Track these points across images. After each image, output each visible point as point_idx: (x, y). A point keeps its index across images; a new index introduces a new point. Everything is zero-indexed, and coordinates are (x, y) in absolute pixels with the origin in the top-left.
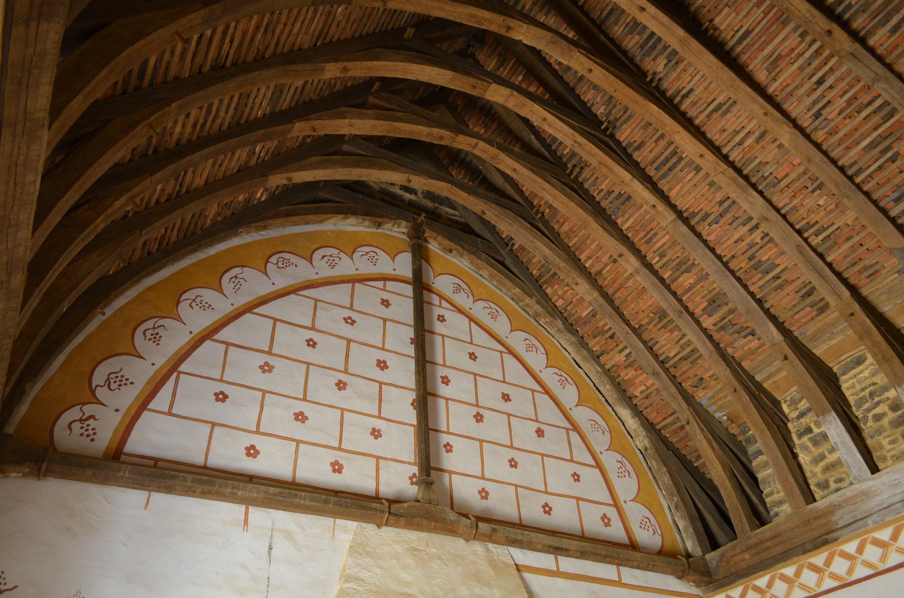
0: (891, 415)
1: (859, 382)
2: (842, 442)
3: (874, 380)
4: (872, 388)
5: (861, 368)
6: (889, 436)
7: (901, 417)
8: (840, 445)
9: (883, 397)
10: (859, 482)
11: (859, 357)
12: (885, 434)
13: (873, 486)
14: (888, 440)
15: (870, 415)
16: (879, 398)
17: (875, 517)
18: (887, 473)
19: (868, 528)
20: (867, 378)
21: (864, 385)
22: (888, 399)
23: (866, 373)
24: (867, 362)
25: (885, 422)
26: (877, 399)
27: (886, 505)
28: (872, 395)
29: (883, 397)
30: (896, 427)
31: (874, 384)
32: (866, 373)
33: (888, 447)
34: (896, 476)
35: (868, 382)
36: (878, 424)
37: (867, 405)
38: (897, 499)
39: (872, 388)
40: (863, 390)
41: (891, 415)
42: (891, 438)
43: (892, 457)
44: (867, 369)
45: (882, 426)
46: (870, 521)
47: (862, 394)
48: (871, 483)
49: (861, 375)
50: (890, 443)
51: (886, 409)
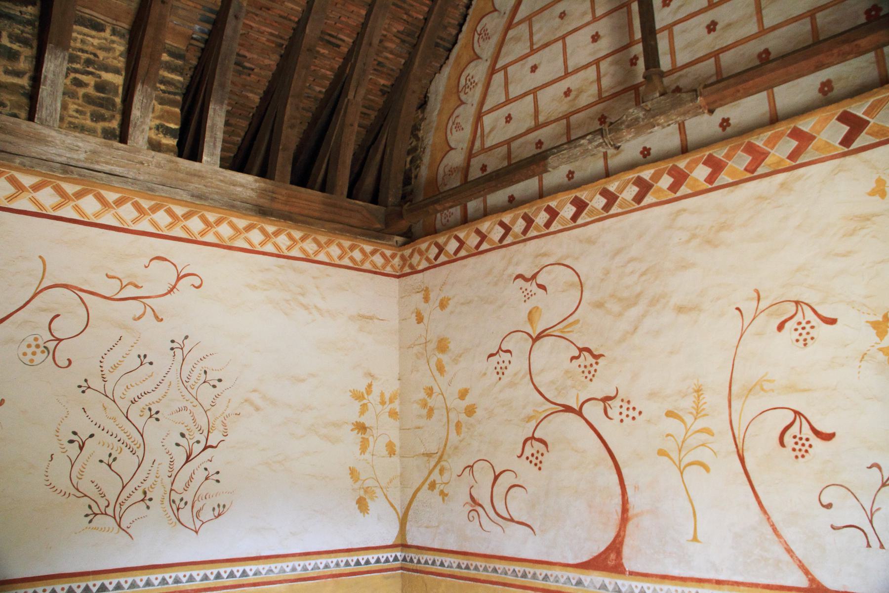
0: (91, 90)
1: (82, 41)
2: (53, 81)
3: (99, 52)
4: (92, 57)
5: (94, 33)
6: (79, 105)
7: (99, 98)
8: (49, 82)
9: (98, 72)
10: (42, 124)
11: (99, 24)
12: (76, 101)
13: (52, 137)
14: (76, 107)
15: (73, 75)
16: (93, 70)
17: (27, 161)
18: (76, 137)
19: (12, 164)
20: (92, 45)
21: (86, 48)
22: (100, 77)
23: (96, 42)
24: (102, 34)
25: (81, 91)
26: (91, 69)
27: (44, 158)
28: (88, 62)
29: (98, 72)
30: (89, 103)
31: (95, 55)
32: (96, 42)
33: (72, 113)
34: (80, 144)
35: (91, 49)
36: (74, 88)
37: (78, 66)
38: (59, 159)
39: (92, 57)
40: (83, 51)
41: (91, 90)
42: (80, 108)
43: (70, 123)
44: (99, 39)
45: (77, 93)
46: (18, 160)
47: (79, 54)
48: (53, 133)
49: (89, 38)
50: (77, 111)
51: (92, 83)
